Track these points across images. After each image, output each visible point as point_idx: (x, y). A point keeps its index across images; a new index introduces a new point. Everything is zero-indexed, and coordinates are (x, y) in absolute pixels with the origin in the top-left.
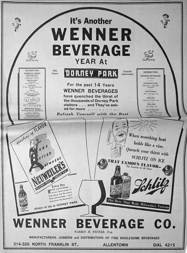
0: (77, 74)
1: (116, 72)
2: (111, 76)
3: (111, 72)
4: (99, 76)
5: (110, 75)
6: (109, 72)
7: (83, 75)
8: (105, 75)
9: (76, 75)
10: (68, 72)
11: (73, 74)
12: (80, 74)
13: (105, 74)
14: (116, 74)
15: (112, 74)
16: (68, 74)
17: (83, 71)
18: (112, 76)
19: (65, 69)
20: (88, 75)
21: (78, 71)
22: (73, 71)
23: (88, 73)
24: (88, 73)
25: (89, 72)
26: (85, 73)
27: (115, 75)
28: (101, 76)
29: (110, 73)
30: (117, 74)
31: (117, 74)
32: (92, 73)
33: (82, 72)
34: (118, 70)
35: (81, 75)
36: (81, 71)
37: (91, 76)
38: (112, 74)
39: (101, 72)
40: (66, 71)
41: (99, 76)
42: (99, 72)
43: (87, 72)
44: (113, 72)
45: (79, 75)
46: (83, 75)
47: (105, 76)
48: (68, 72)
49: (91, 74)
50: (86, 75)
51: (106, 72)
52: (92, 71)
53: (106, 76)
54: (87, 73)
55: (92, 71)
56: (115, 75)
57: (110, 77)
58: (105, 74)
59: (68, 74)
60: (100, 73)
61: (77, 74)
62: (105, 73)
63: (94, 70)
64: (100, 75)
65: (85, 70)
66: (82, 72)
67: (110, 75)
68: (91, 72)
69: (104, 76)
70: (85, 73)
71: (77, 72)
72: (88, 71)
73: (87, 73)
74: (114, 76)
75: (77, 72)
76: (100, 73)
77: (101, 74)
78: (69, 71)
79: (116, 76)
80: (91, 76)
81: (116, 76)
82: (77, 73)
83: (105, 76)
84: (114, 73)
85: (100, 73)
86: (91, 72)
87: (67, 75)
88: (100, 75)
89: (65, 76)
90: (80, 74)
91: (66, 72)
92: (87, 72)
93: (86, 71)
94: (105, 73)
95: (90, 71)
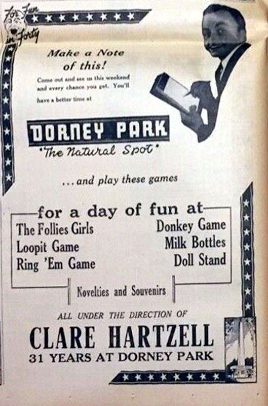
0: (63, 135)
1: (163, 122)
2: (151, 134)
3: (150, 123)
4: (119, 136)
5: (147, 132)
6: (145, 123)
7: (78, 138)
8: (134, 133)
9: (60, 138)
10: (37, 130)
11: (50, 136)
12: (69, 133)
13: (134, 129)
14: (163, 129)
15: (154, 131)
16: (38, 136)
17: (78, 126)
18: (153, 135)
19: (30, 123)
20: (89, 138)
21: (64, 127)
22: (52, 127)
23: (89, 132)
24: (89, 132)
25: (92, 128)
26: (82, 132)
27: (160, 132)
28: (126, 136)
29: (147, 126)
30: (167, 130)
31: (167, 130)
32: (102, 130)
33: (75, 130)
34: (168, 116)
35: (73, 138)
36: (72, 126)
37: (99, 137)
38: (154, 131)
39: (124, 124)
40: (32, 127)
41: (119, 136)
42: (119, 124)
43: (88, 128)
44: (157, 122)
45: (66, 138)
46: (78, 138)
47: (134, 136)
48: (37, 130)
49: (99, 132)
50: (86, 137)
51: (137, 124)
52: (102, 125)
53: (138, 135)
54: (86, 132)
55: (102, 125)
56: (160, 132)
57: (148, 138)
58: (134, 129)
59: (38, 136)
60: (121, 127)
61: (63, 135)
62: (134, 127)
63: (106, 121)
64: (122, 133)
65: (81, 122)
66: (75, 130)
67: (147, 132)
68: (99, 128)
69: (131, 136)
70: (82, 132)
71: (62, 129)
72: (89, 125)
73: (86, 131)
74: (158, 134)
75: (62, 129)
76: (121, 127)
77: (124, 130)
78: (40, 127)
79: (164, 133)
80: (99, 137)
81: (164, 133)
82: (62, 133)
83: (134, 136)
84: (160, 126)
85: (121, 128)
86: (99, 128)
87: (35, 139)
88: (122, 133)
89: (32, 143)
90: (69, 133)
91: (32, 130)
92: (88, 128)
93: (85, 126)
94: (134, 127)
95: (96, 125)
